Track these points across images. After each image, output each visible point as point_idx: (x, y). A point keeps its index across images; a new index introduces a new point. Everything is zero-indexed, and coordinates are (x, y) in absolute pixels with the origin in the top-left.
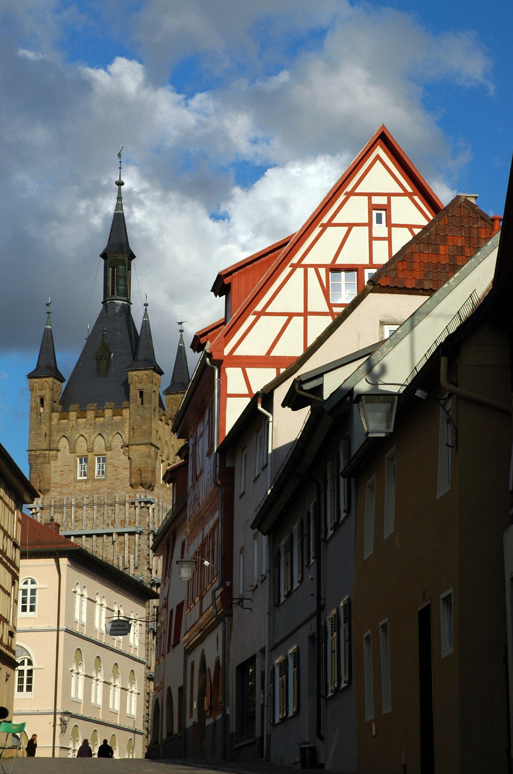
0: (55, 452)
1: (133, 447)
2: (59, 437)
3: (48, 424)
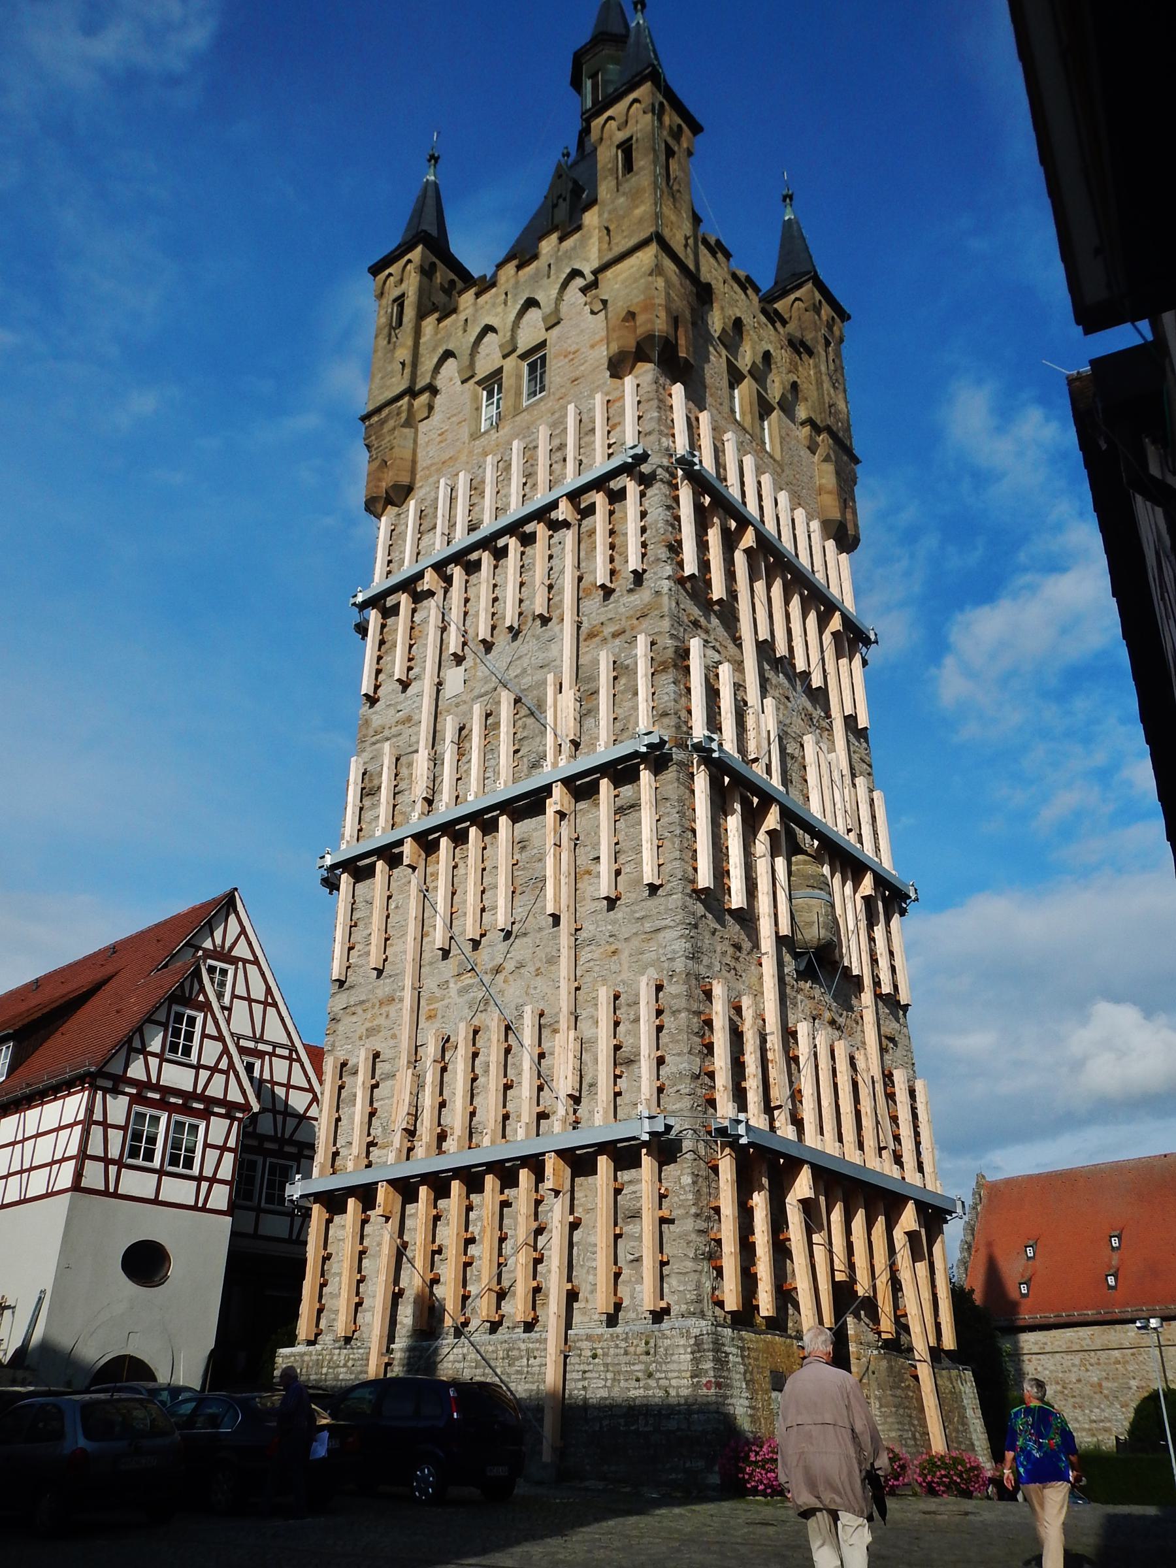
0: (424, 398)
1: (609, 273)
2: (435, 360)
3: (410, 342)
